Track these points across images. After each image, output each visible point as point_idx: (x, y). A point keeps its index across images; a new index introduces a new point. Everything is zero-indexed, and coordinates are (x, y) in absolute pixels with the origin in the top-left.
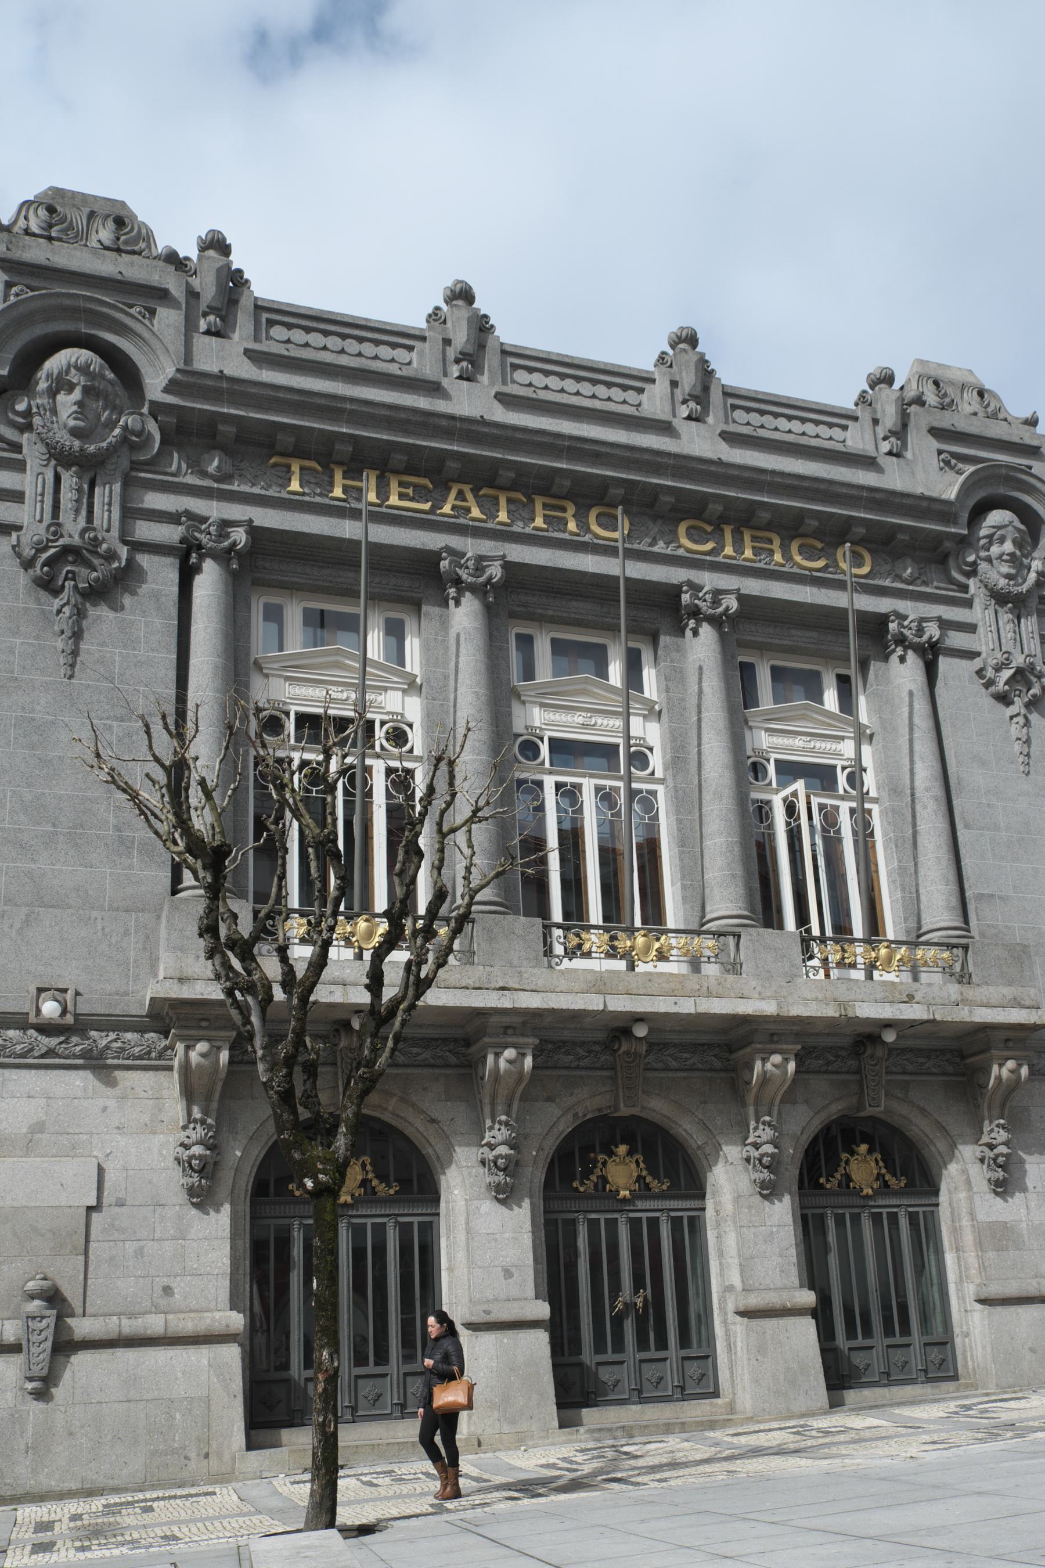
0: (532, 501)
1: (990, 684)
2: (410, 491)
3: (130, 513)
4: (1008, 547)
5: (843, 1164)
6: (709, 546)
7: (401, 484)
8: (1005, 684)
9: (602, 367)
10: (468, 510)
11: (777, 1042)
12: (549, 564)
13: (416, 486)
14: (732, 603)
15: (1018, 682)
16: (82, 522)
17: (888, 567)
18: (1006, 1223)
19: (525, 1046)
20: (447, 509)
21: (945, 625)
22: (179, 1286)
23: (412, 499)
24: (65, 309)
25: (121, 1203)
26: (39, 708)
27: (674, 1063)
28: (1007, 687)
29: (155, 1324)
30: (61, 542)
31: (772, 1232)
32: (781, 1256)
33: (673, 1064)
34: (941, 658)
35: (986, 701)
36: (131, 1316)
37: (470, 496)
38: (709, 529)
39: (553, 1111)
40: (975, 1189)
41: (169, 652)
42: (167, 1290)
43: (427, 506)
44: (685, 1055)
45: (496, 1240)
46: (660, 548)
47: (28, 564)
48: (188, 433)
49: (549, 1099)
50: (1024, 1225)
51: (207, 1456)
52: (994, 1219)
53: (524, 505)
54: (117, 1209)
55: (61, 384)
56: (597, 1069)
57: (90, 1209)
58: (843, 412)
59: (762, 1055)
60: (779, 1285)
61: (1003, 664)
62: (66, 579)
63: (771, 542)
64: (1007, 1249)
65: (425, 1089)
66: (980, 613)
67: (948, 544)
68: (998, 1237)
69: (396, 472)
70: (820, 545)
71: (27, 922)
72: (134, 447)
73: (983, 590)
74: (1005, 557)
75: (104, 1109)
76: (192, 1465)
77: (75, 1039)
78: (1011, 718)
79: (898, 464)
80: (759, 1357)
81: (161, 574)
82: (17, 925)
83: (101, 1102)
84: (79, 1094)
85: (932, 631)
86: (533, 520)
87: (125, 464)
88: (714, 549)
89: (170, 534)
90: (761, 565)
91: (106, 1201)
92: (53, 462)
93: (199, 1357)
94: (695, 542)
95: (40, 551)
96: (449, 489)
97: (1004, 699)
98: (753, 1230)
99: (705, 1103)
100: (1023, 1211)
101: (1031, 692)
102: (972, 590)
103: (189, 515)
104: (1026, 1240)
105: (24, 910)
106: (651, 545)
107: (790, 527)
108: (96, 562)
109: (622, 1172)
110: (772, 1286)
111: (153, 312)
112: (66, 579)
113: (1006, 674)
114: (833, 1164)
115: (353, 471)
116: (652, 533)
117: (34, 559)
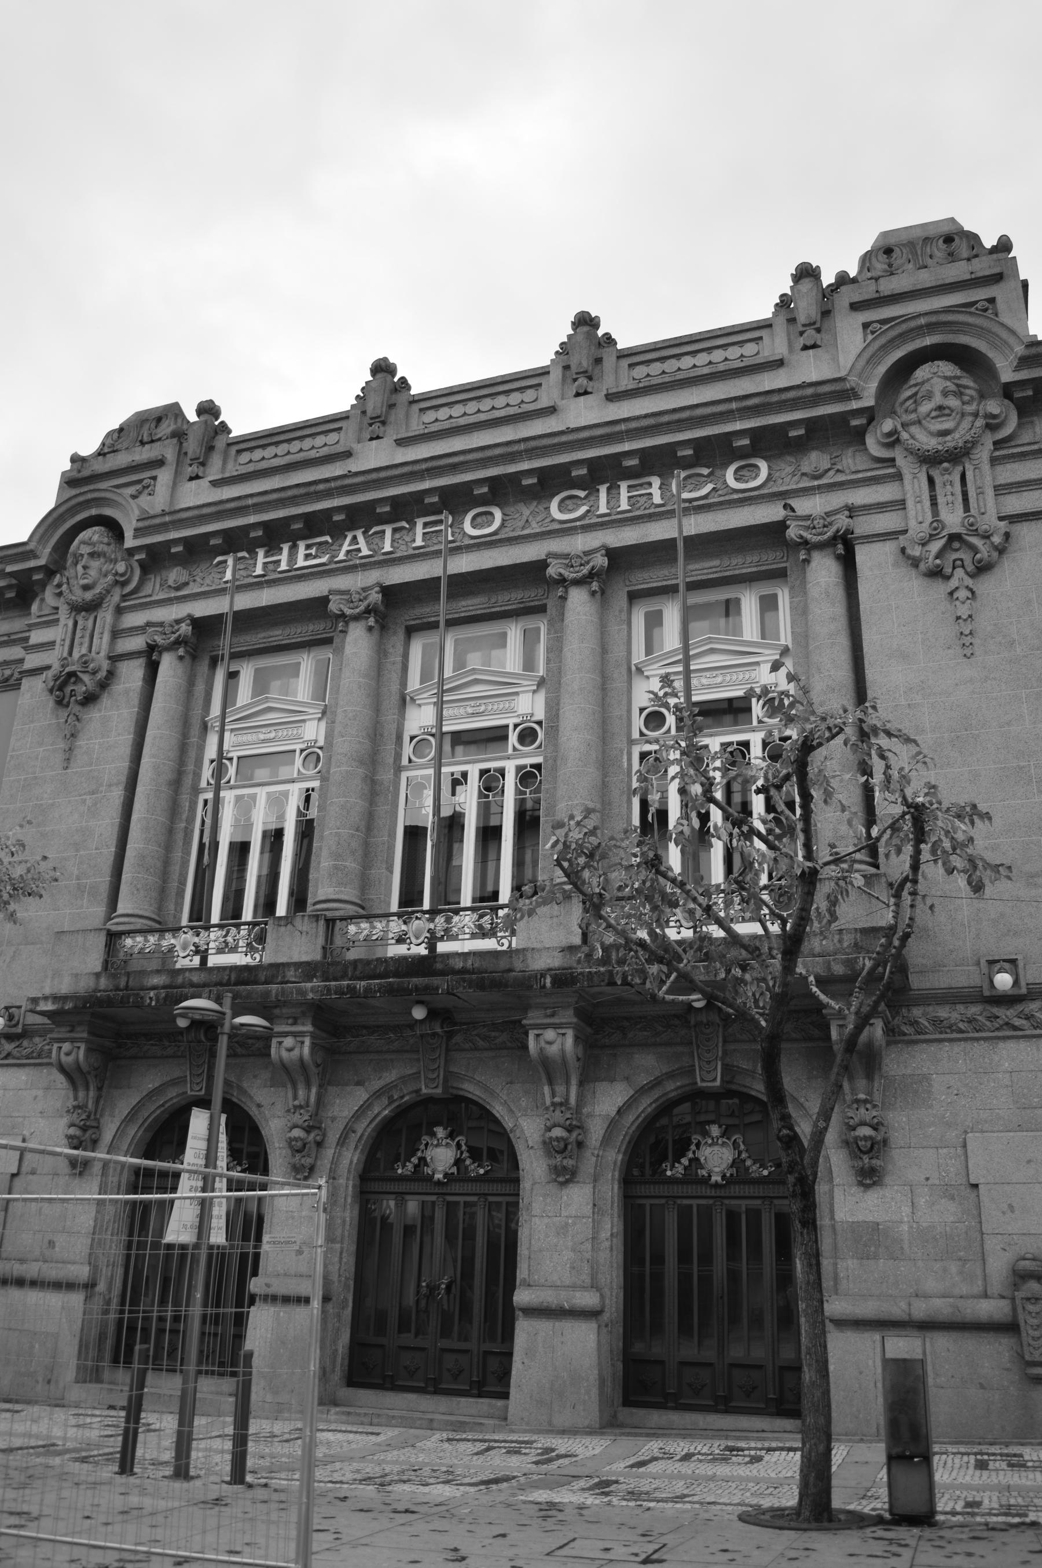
0: (413, 525)
1: (915, 562)
2: (313, 551)
3: (116, 634)
4: (938, 399)
5: (693, 1147)
6: (583, 509)
7: (308, 547)
8: (936, 558)
9: (499, 380)
10: (359, 550)
11: (553, 1015)
12: (427, 577)
13: (320, 544)
14: (601, 561)
15: (957, 550)
16: (84, 651)
17: (789, 469)
18: (878, 1224)
19: (302, 1034)
20: (341, 556)
21: (852, 511)
22: (60, 1240)
23: (315, 557)
24: (80, 504)
25: (33, 1172)
26: (46, 796)
27: (481, 1042)
28: (938, 561)
29: (32, 1270)
30: (67, 670)
31: (567, 1224)
32: (574, 1250)
33: (481, 1043)
34: (857, 548)
35: (914, 584)
36: (22, 1261)
37: (361, 539)
38: (582, 494)
39: (360, 1095)
40: (837, 1181)
41: (129, 734)
42: (51, 1244)
43: (324, 560)
44: (493, 1034)
45: (293, 1218)
46: (535, 528)
47: (51, 691)
48: (155, 559)
49: (359, 1083)
50: (906, 1228)
51: (49, 1382)
52: (861, 1218)
53: (410, 530)
54: (31, 1177)
55: (77, 558)
56: (407, 1051)
57: (13, 1175)
58: (755, 325)
59: (536, 1032)
60: (567, 1283)
61: (931, 535)
62: (71, 696)
63: (650, 484)
64: (876, 1257)
65: (255, 1077)
66: (914, 484)
67: (855, 423)
68: (872, 1239)
69: (304, 538)
70: (705, 471)
71: (13, 958)
72: (124, 584)
73: (910, 458)
74: (934, 414)
75: (35, 1098)
76: (39, 1387)
77: (25, 1043)
78: (951, 594)
79: (814, 356)
80: (526, 1361)
81: (132, 674)
82: (8, 960)
83: (34, 1092)
84: (23, 1087)
85: (842, 522)
86: (414, 541)
87: (116, 598)
88: (588, 511)
89: (137, 643)
90: (638, 513)
91: (24, 1169)
92: (73, 614)
93: (54, 1300)
94: (571, 511)
95: (56, 680)
96: (346, 537)
97: (936, 574)
98: (546, 1220)
99: (511, 1083)
100: (906, 1210)
101: (978, 556)
102: (900, 461)
103: (149, 624)
104: (906, 1246)
105: (13, 949)
106: (523, 528)
107: (658, 462)
108: (86, 678)
109: (441, 1157)
110: (559, 1283)
111: (154, 478)
112: (71, 696)
113: (936, 546)
114: (682, 1147)
115: (273, 548)
116: (525, 518)
117: (53, 687)
